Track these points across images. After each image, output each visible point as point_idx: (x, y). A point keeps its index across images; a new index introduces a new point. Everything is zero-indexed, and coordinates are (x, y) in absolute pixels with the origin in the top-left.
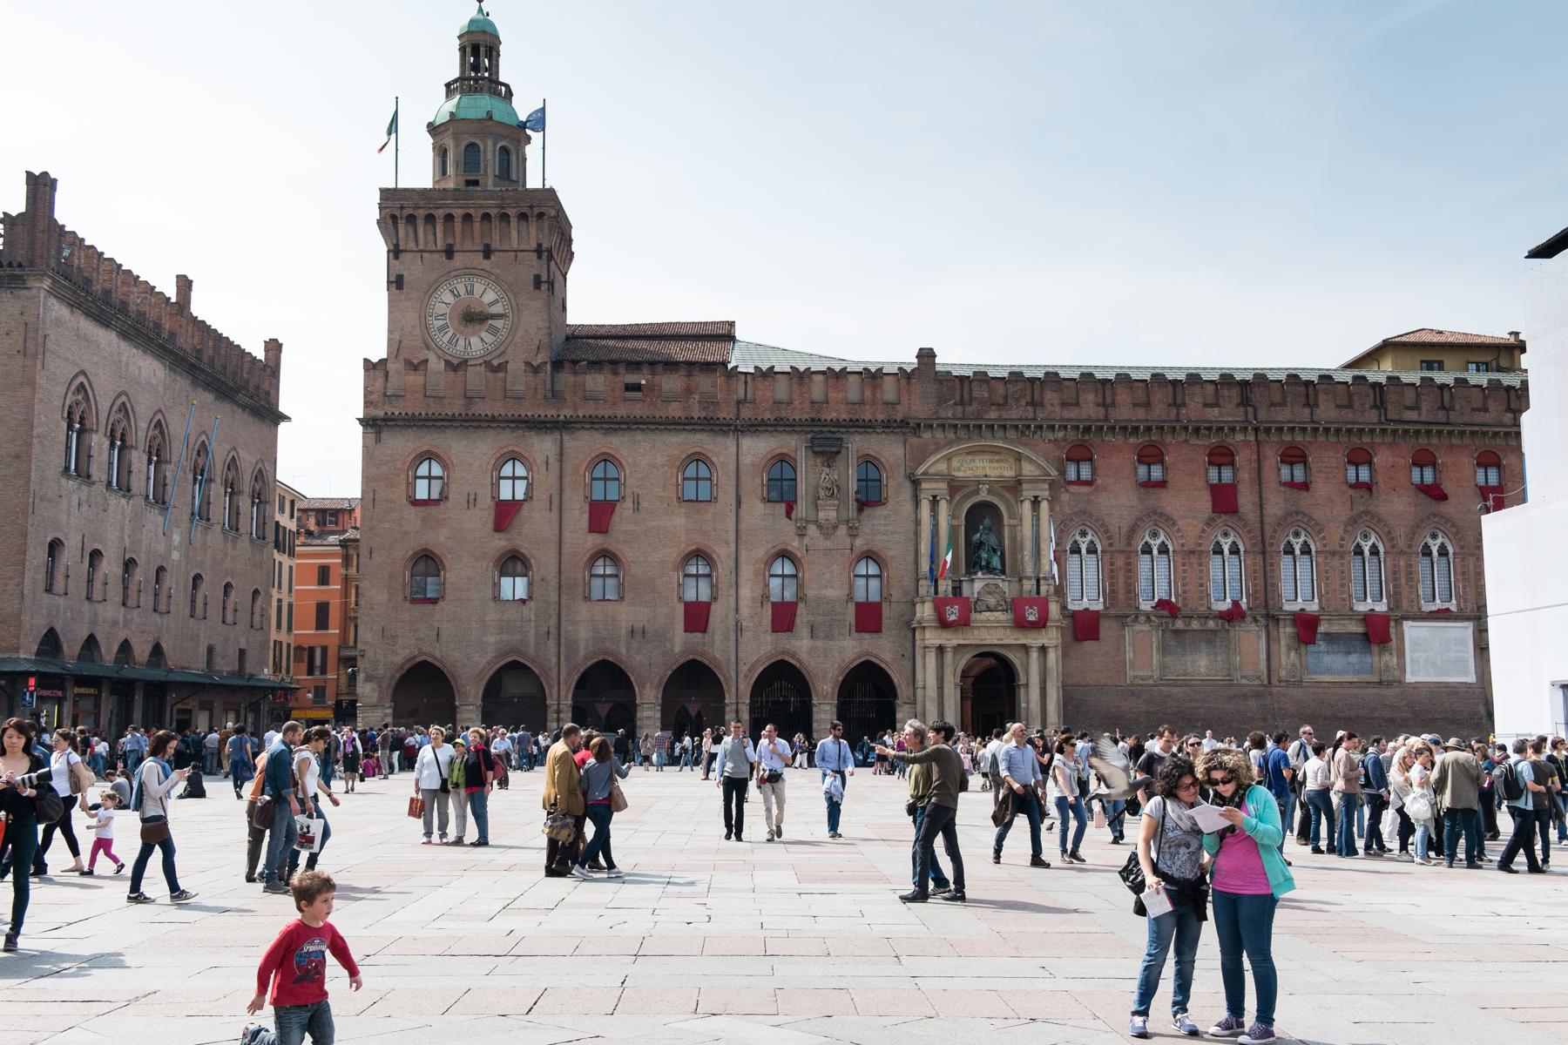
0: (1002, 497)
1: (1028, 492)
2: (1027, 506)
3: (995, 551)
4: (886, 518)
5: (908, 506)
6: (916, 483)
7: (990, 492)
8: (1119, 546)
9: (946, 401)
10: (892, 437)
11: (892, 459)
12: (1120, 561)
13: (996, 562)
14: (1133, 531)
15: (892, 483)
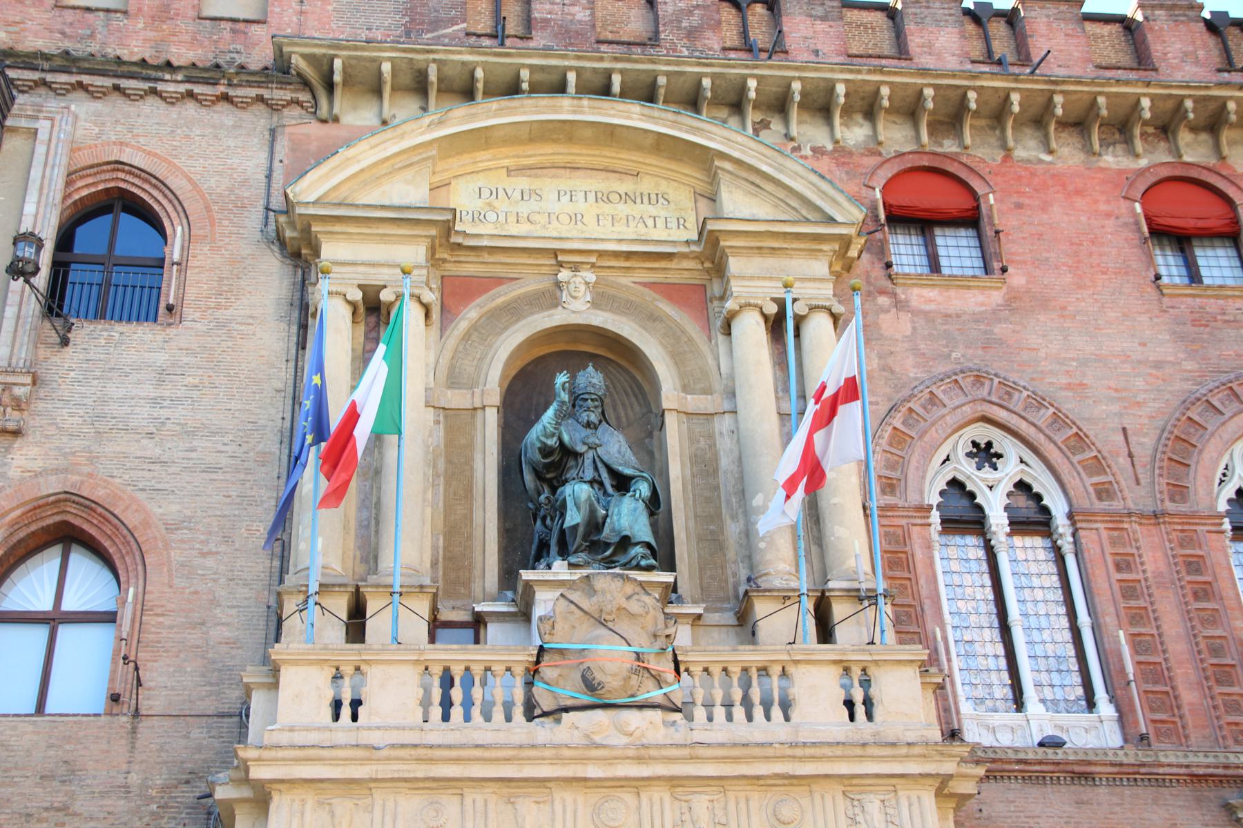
0: (651, 319)
1: (752, 281)
2: (751, 330)
3: (623, 483)
4: (162, 376)
5: (270, 338)
6: (298, 250)
7: (600, 300)
8: (1134, 497)
9: (436, 24)
10: (224, 116)
11: (215, 184)
12: (1153, 554)
13: (627, 515)
14: (1180, 448)
15: (202, 256)
